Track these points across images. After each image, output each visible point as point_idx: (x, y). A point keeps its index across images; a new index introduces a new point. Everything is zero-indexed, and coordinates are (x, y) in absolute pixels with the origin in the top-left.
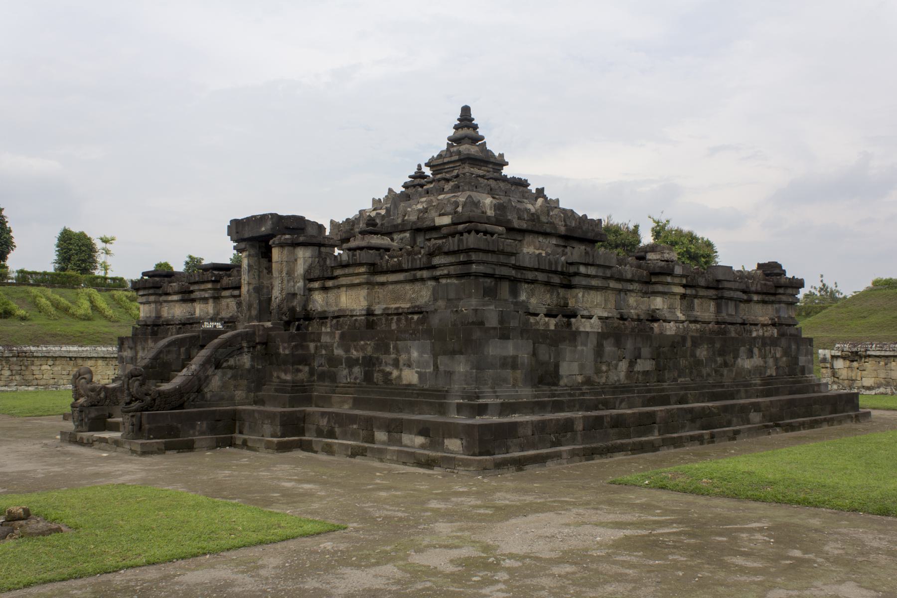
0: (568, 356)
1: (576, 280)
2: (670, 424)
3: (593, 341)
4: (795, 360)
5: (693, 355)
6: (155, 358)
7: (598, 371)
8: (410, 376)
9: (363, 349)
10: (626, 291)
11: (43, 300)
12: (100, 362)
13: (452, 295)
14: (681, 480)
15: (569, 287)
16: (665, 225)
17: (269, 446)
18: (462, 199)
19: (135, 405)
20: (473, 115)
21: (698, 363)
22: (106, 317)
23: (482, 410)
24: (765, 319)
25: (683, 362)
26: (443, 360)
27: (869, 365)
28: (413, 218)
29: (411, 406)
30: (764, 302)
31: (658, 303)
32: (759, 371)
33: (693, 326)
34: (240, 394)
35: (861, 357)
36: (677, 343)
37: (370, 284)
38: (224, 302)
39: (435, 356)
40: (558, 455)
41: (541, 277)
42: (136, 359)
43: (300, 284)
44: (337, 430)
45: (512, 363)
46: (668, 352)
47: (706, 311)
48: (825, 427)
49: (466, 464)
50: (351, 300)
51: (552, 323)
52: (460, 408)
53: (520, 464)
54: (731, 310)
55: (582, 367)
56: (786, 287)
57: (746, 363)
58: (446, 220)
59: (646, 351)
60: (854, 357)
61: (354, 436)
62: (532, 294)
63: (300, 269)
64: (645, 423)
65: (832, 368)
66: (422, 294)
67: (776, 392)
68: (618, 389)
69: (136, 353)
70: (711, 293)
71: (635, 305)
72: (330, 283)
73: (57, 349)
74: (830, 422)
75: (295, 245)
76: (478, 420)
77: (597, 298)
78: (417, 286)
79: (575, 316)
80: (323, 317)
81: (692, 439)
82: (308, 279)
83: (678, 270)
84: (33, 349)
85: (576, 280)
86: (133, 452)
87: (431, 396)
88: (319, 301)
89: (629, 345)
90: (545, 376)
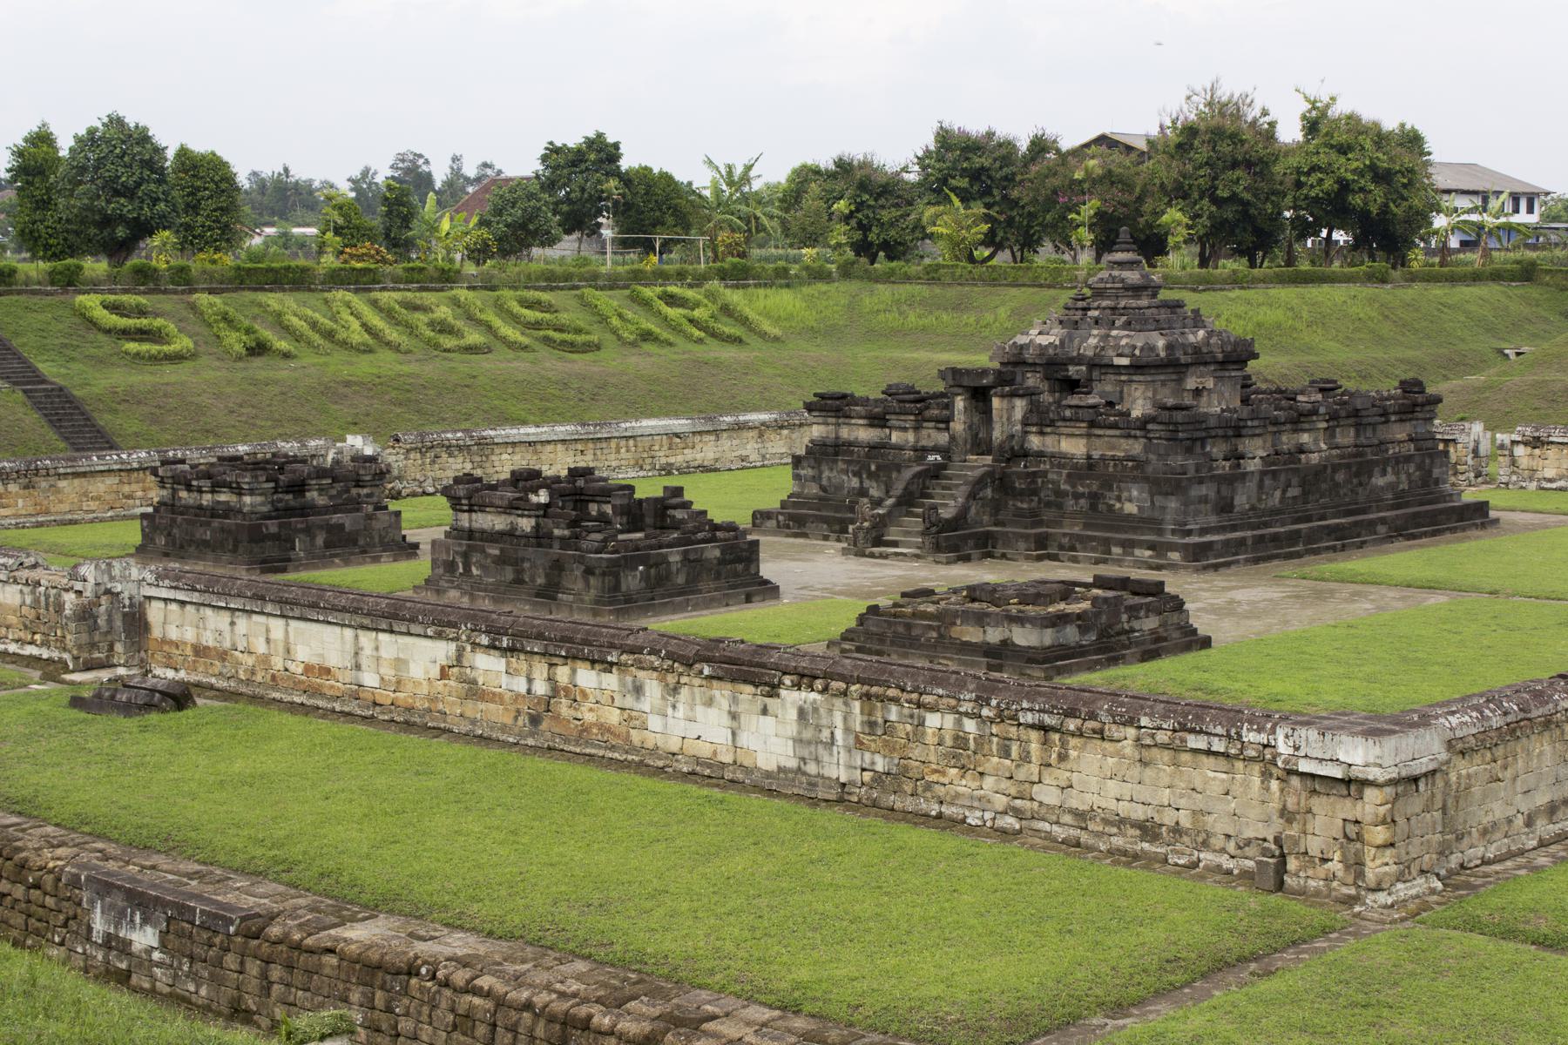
0: (1240, 491)
1: (1244, 432)
2: (1312, 537)
3: (1257, 477)
4: (1430, 472)
5: (1333, 479)
6: (906, 489)
7: (1260, 500)
8: (1131, 508)
9: (1088, 486)
10: (1280, 432)
11: (295, 320)
12: (560, 447)
13: (1162, 452)
14: (1315, 574)
15: (1240, 436)
16: (1328, 106)
17: (1028, 558)
18: (1139, 344)
19: (934, 529)
21: (1337, 485)
22: (388, 344)
23: (1189, 533)
24: (1402, 436)
25: (1324, 486)
26: (1159, 500)
27: (1552, 453)
28: (1090, 353)
29: (1135, 530)
30: (1401, 420)
31: (1305, 438)
32: (1392, 486)
33: (1334, 452)
34: (986, 518)
35: (1543, 444)
36: (1319, 471)
37: (1089, 436)
38: (924, 432)
39: (1152, 496)
40: (1237, 562)
41: (1220, 432)
42: (820, 478)
43: (1019, 427)
44: (1078, 546)
45: (1204, 500)
46: (1313, 479)
47: (1346, 437)
48: (1448, 536)
49: (1185, 568)
50: (1073, 446)
51: (1227, 464)
52: (1173, 532)
53: (1216, 567)
54: (1369, 433)
55: (1249, 498)
56: (1423, 405)
57: (1379, 481)
58: (1125, 361)
59: (1295, 481)
60: (1536, 443)
61: (1093, 550)
62: (1213, 445)
63: (1018, 414)
64: (1293, 538)
65: (1512, 455)
66: (1136, 447)
67: (1407, 505)
68: (1274, 512)
69: (821, 473)
70: (1351, 421)
71: (1287, 441)
72: (1049, 430)
73: (515, 431)
74: (1453, 530)
75: (1013, 395)
76: (1187, 540)
77: (1259, 442)
78: (1131, 441)
79: (1243, 458)
80: (1040, 454)
81: (1328, 548)
82: (1025, 423)
83: (1322, 410)
84: (492, 433)
85: (1244, 432)
86: (937, 563)
87: (1147, 522)
88: (1035, 442)
89: (1283, 478)
90: (1225, 507)
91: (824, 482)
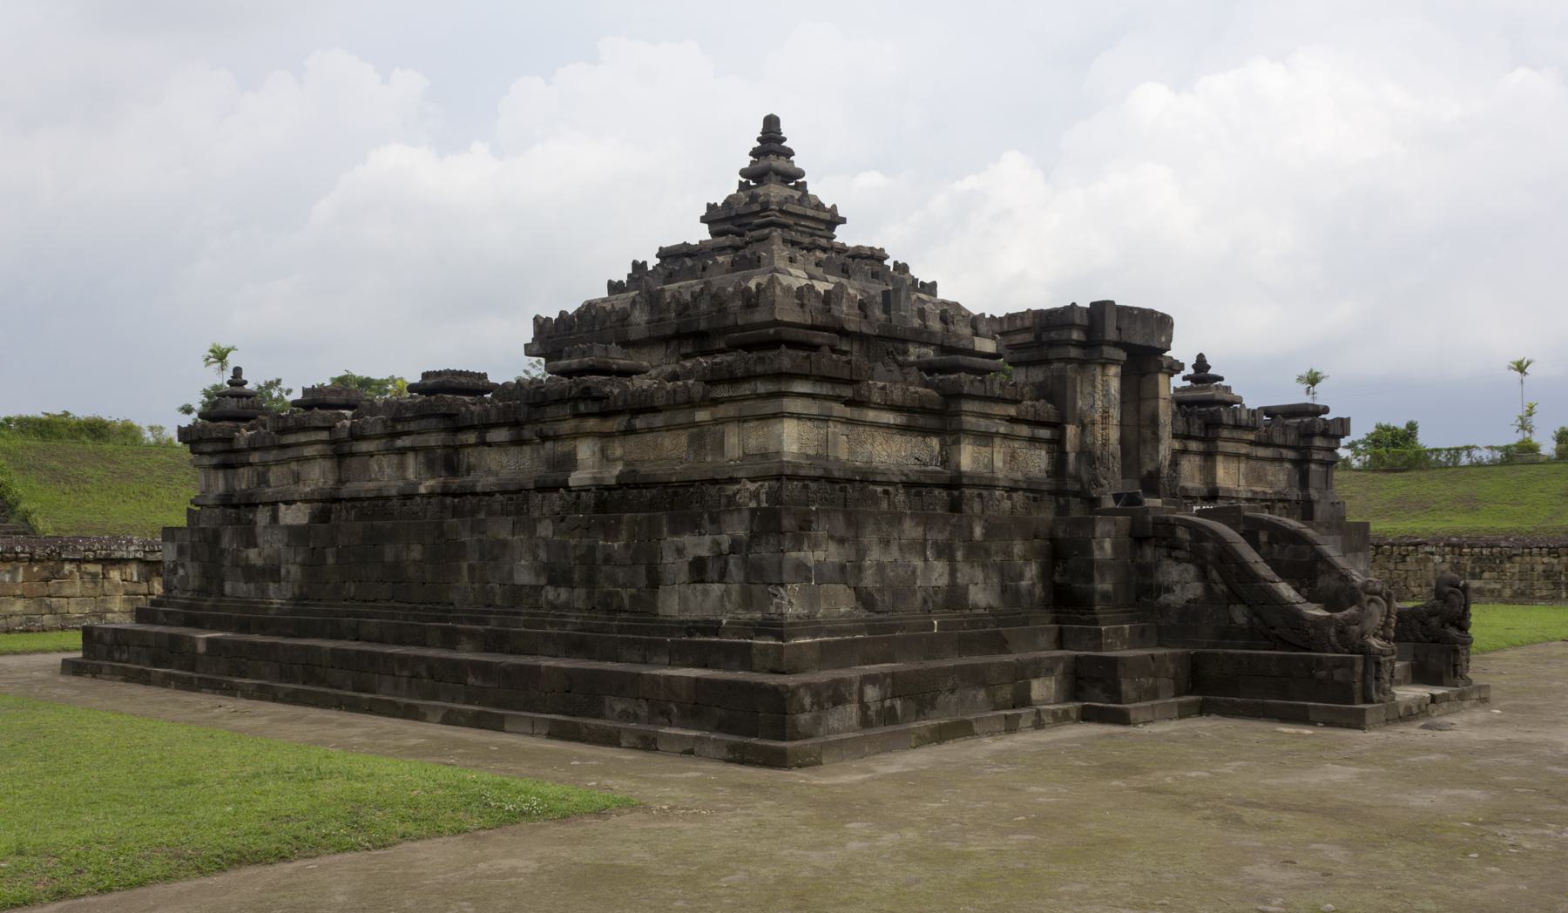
20: (785, 129)
42: (859, 569)
69: (861, 554)
91: (869, 580)
